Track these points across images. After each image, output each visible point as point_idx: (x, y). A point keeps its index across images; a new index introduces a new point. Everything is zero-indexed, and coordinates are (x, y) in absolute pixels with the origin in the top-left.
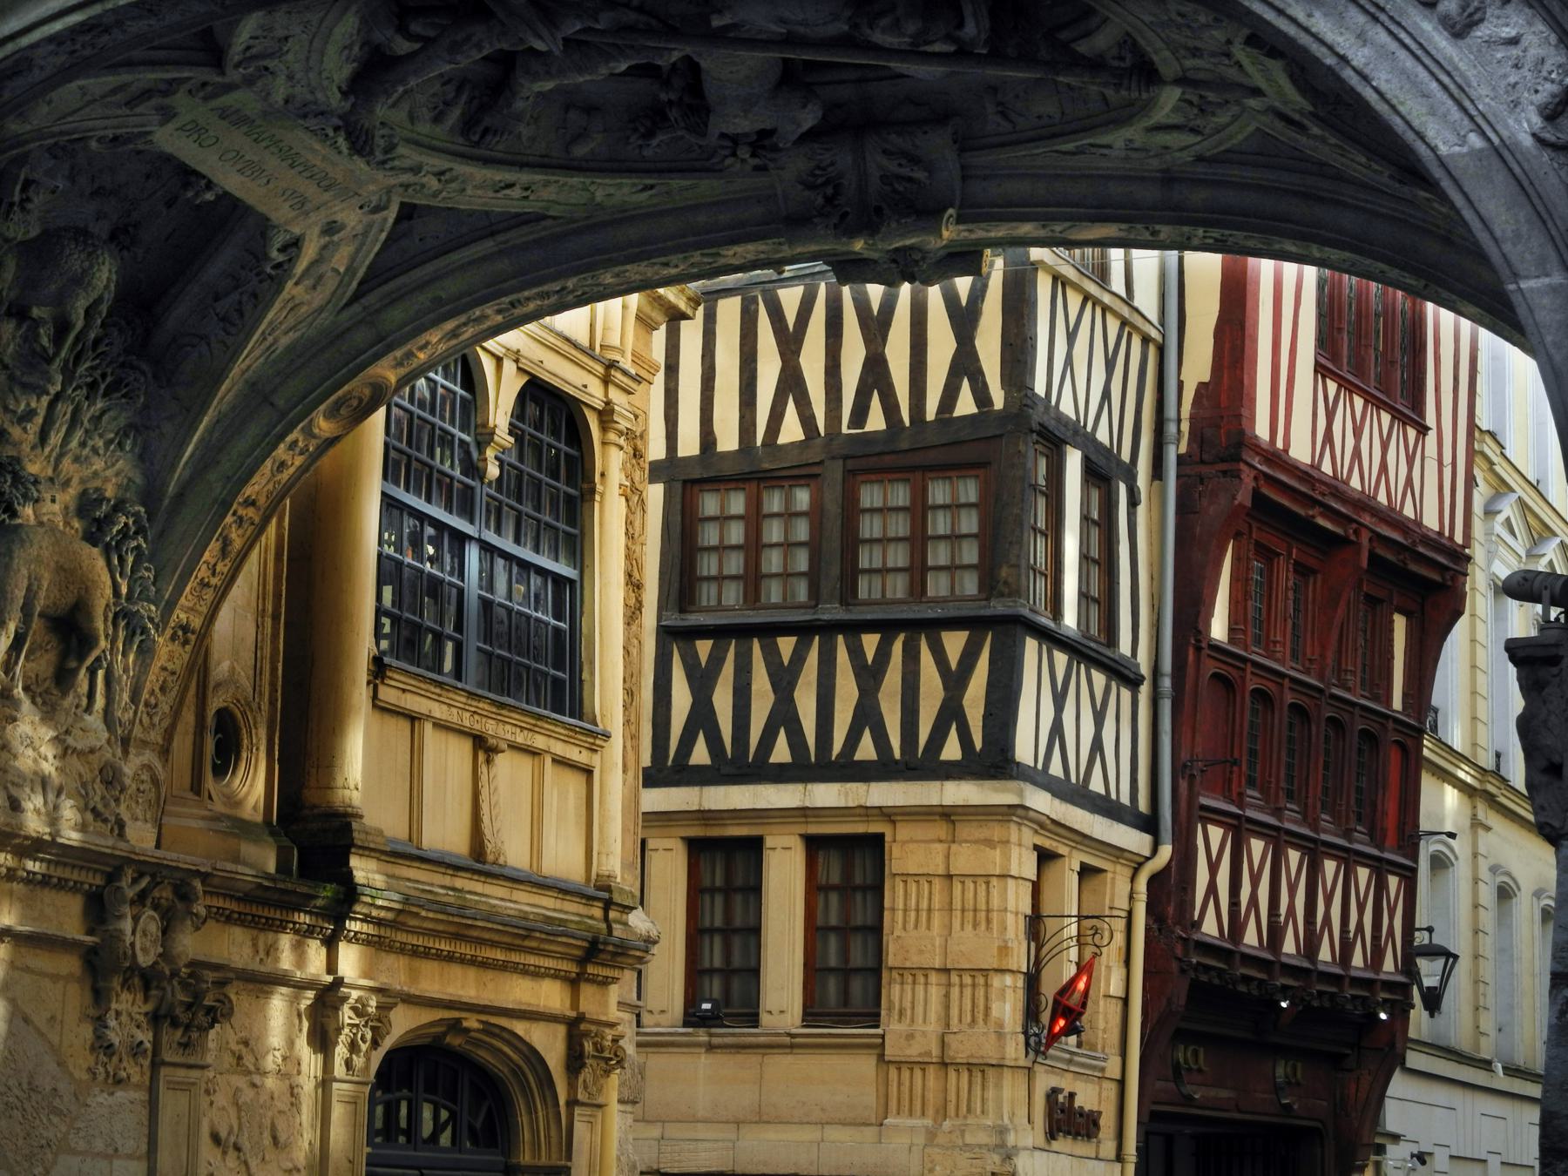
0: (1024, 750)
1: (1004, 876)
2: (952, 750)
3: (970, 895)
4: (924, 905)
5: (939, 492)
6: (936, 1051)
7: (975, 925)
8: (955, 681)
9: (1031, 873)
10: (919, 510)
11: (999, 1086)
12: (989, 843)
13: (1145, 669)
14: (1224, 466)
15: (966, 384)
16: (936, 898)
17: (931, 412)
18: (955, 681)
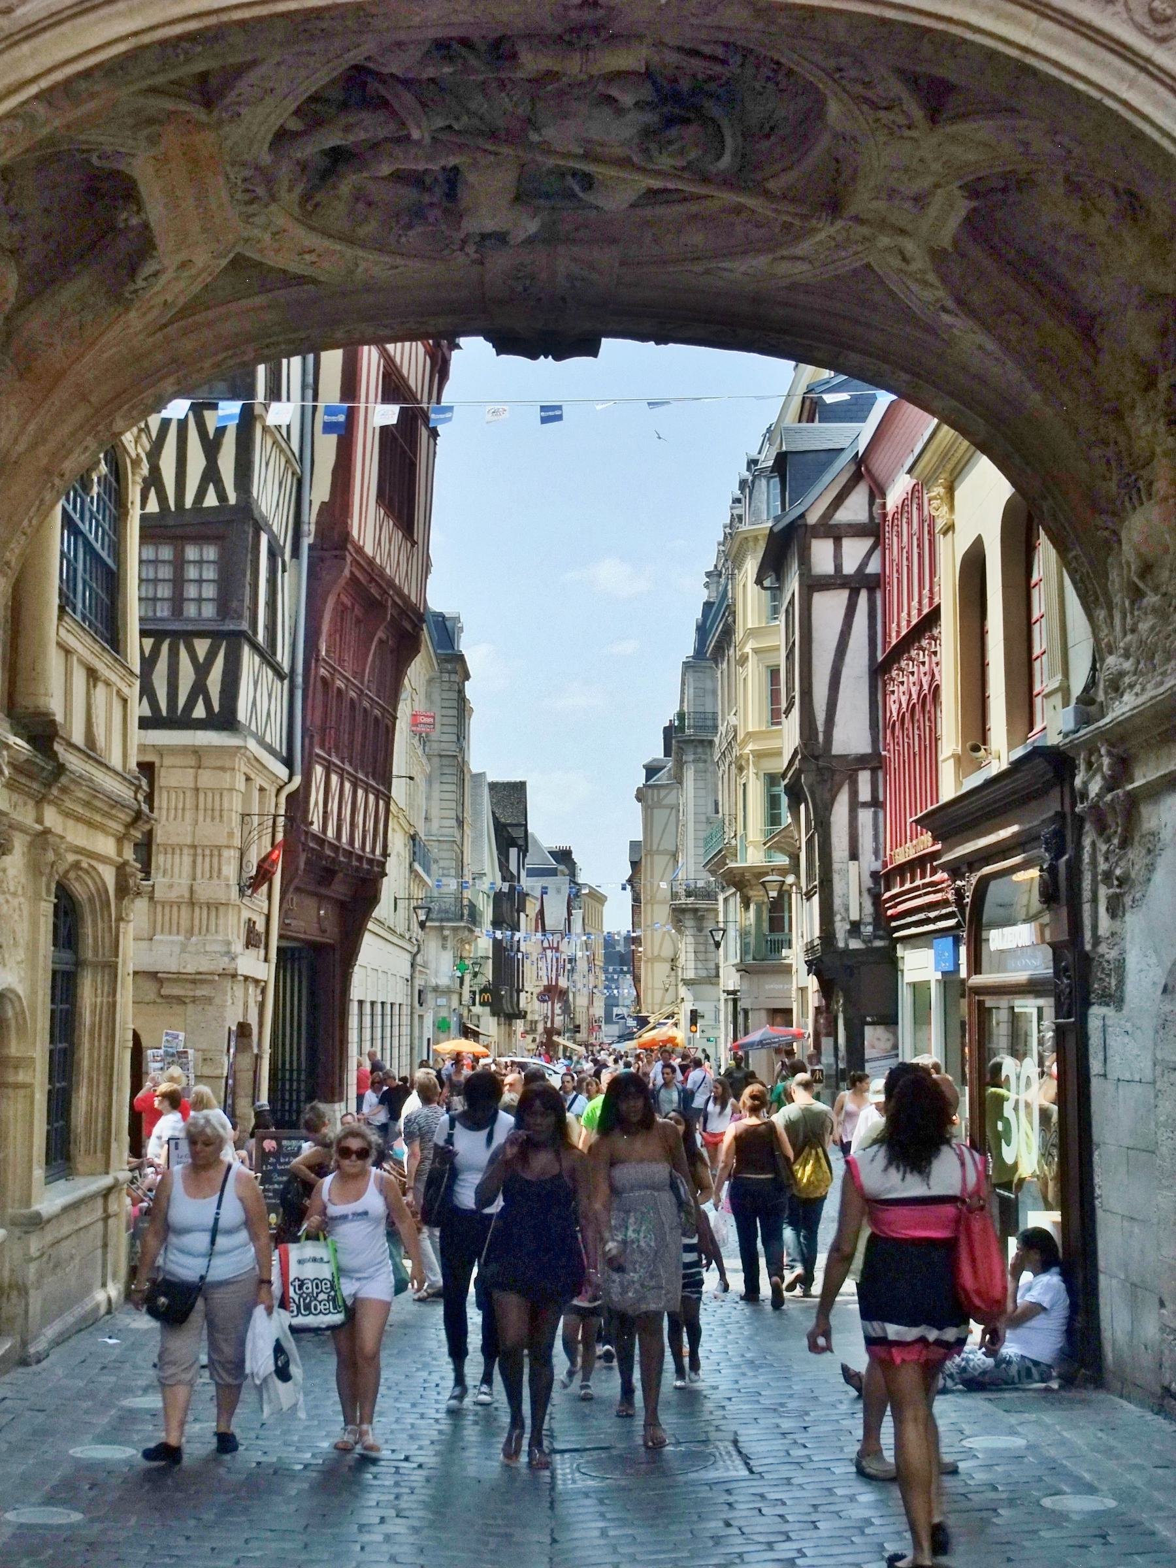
0: (242, 715)
1: (231, 790)
2: (199, 712)
3: (210, 799)
4: (180, 806)
5: (191, 553)
6: (187, 895)
7: (213, 819)
8: (202, 670)
9: (243, 789)
10: (179, 564)
11: (226, 915)
12: (222, 769)
13: (286, 669)
14: (337, 553)
15: (211, 488)
16: (188, 801)
17: (188, 504)
18: (202, 670)
